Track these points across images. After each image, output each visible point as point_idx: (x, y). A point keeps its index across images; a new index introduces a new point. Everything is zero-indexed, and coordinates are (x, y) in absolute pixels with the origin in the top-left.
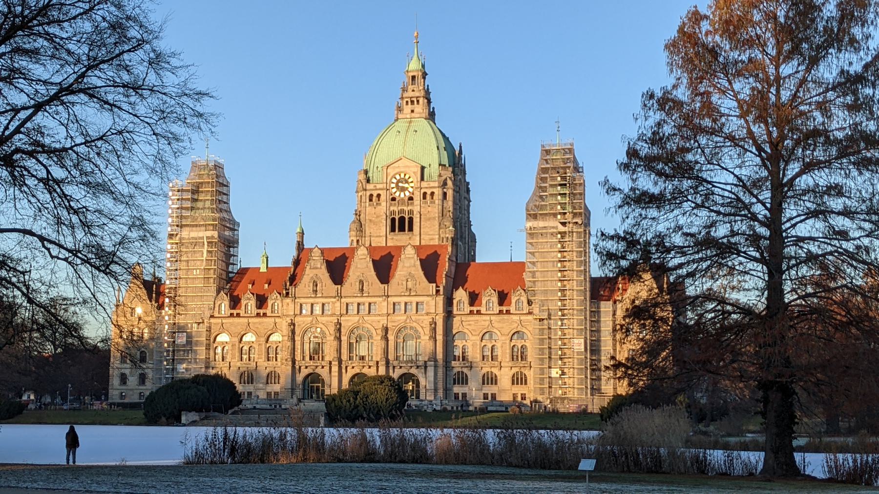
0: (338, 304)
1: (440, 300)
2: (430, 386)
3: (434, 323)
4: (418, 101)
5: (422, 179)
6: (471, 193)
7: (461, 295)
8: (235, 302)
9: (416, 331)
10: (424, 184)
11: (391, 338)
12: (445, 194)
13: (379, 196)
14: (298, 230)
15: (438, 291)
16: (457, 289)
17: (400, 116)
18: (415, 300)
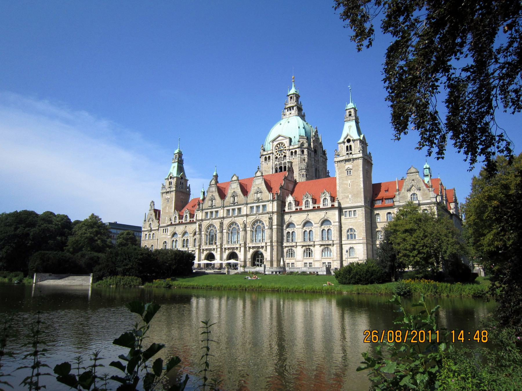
0: (222, 211)
1: (275, 203)
2: (269, 259)
3: (271, 219)
4: (293, 109)
5: (290, 144)
6: (327, 155)
7: (290, 199)
8: (181, 217)
9: (263, 224)
10: (291, 147)
11: (248, 229)
12: (303, 152)
13: (269, 157)
14: (215, 174)
15: (274, 198)
16: (288, 196)
17: (284, 117)
18: (261, 204)
